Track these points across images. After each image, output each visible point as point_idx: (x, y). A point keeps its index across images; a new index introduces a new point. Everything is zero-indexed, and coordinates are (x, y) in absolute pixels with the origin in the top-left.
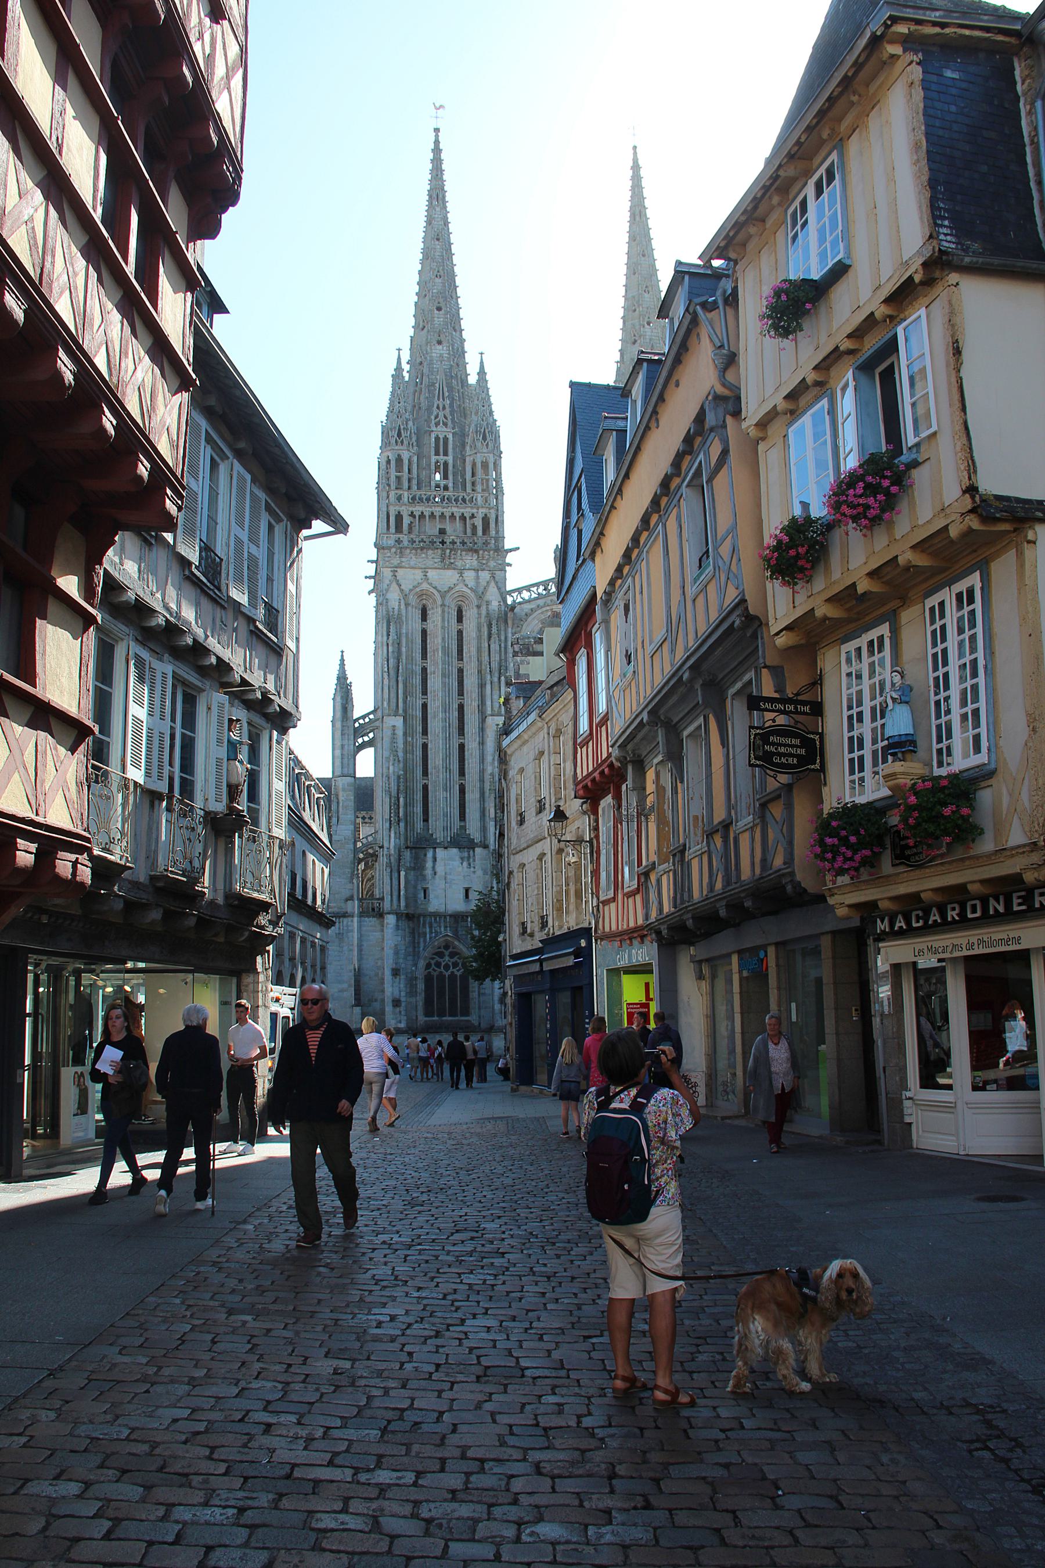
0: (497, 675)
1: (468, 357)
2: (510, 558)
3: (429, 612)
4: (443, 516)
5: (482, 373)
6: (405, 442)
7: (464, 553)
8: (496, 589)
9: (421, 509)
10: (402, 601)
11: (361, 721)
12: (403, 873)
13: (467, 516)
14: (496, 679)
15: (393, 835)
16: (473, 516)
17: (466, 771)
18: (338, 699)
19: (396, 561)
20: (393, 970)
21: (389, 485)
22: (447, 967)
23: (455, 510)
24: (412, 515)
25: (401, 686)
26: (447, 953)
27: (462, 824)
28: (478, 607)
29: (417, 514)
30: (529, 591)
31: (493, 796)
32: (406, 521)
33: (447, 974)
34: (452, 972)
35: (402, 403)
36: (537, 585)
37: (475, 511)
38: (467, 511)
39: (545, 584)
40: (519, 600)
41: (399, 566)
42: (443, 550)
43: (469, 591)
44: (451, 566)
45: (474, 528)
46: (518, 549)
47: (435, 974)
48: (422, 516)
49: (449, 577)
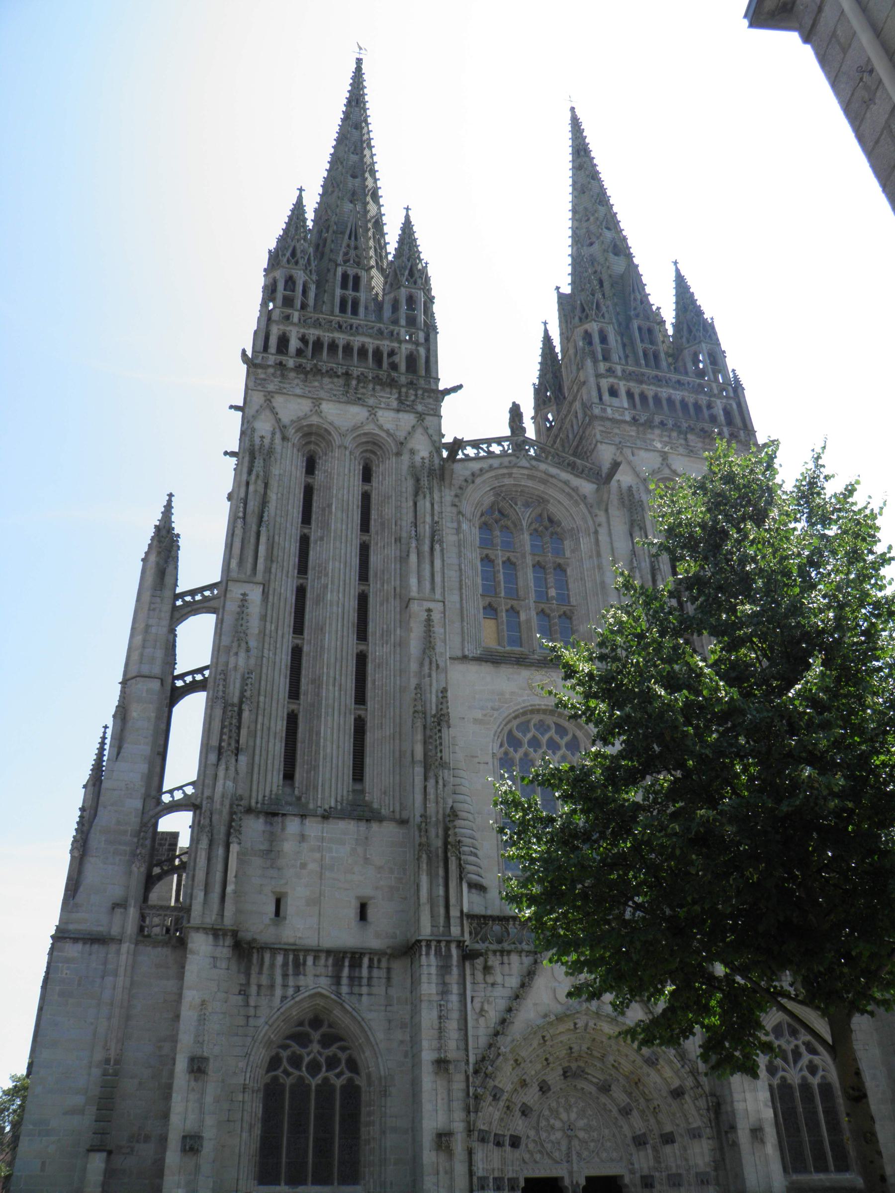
0: (427, 542)
2: (448, 405)
3: (320, 463)
4: (348, 349)
5: (407, 229)
10: (278, 436)
11: (188, 599)
12: (234, 848)
14: (426, 548)
15: (221, 773)
16: (392, 353)
17: (369, 694)
18: (153, 558)
19: (271, 387)
20: (192, 1060)
22: (314, 1068)
23: (367, 340)
24: (303, 339)
25: (263, 539)
26: (316, 1036)
27: (358, 787)
28: (398, 454)
29: (311, 340)
31: (419, 724)
32: (294, 344)
33: (314, 1082)
34: (326, 1080)
36: (489, 441)
38: (386, 345)
39: (499, 441)
41: (280, 392)
43: (384, 435)
44: (359, 401)
45: (394, 367)
46: (460, 387)
47: (289, 1082)
48: (318, 344)
49: (354, 415)
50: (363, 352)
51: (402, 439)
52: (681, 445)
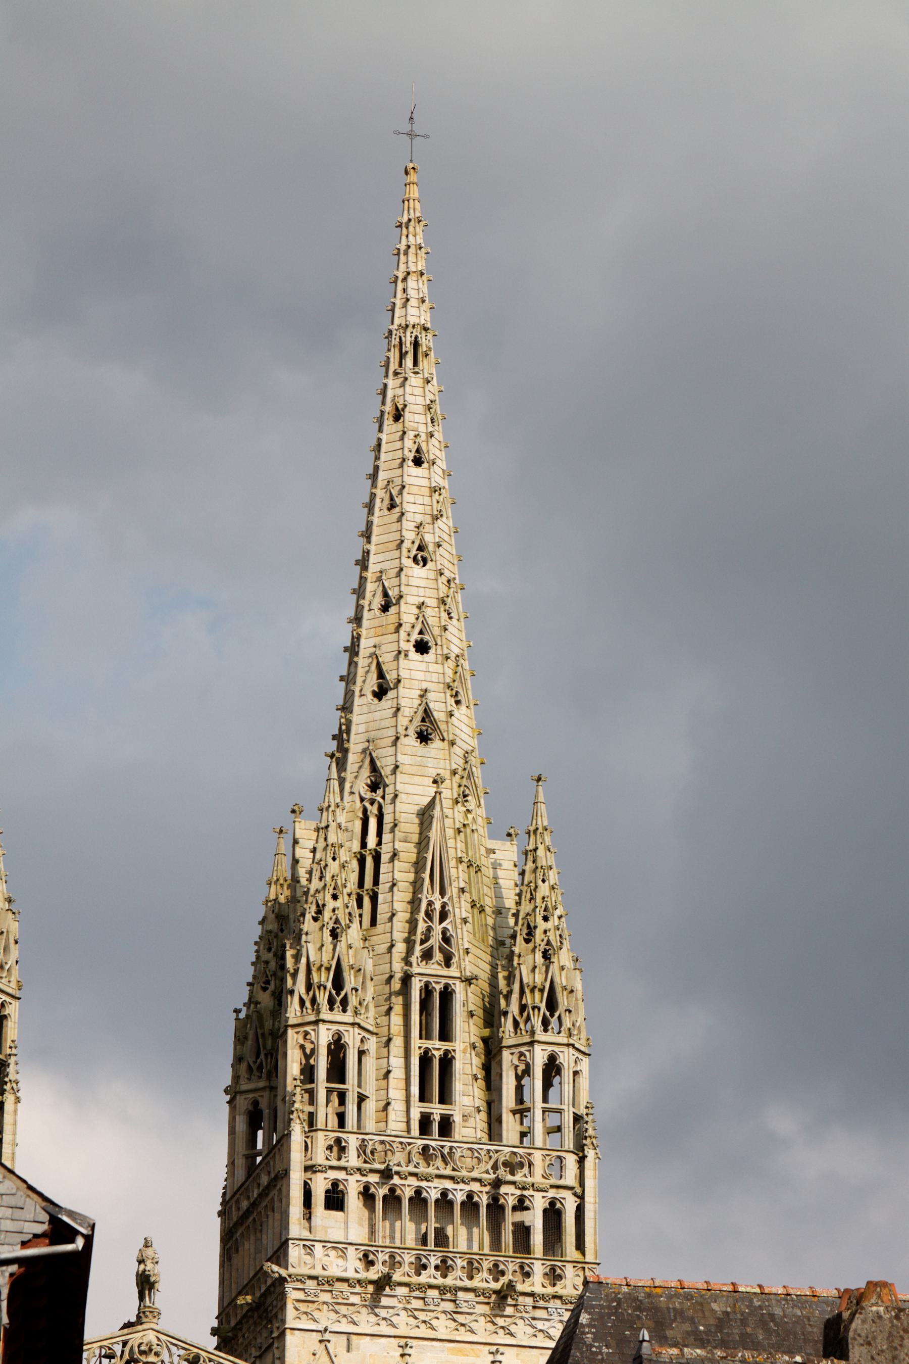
52: (444, 1312)
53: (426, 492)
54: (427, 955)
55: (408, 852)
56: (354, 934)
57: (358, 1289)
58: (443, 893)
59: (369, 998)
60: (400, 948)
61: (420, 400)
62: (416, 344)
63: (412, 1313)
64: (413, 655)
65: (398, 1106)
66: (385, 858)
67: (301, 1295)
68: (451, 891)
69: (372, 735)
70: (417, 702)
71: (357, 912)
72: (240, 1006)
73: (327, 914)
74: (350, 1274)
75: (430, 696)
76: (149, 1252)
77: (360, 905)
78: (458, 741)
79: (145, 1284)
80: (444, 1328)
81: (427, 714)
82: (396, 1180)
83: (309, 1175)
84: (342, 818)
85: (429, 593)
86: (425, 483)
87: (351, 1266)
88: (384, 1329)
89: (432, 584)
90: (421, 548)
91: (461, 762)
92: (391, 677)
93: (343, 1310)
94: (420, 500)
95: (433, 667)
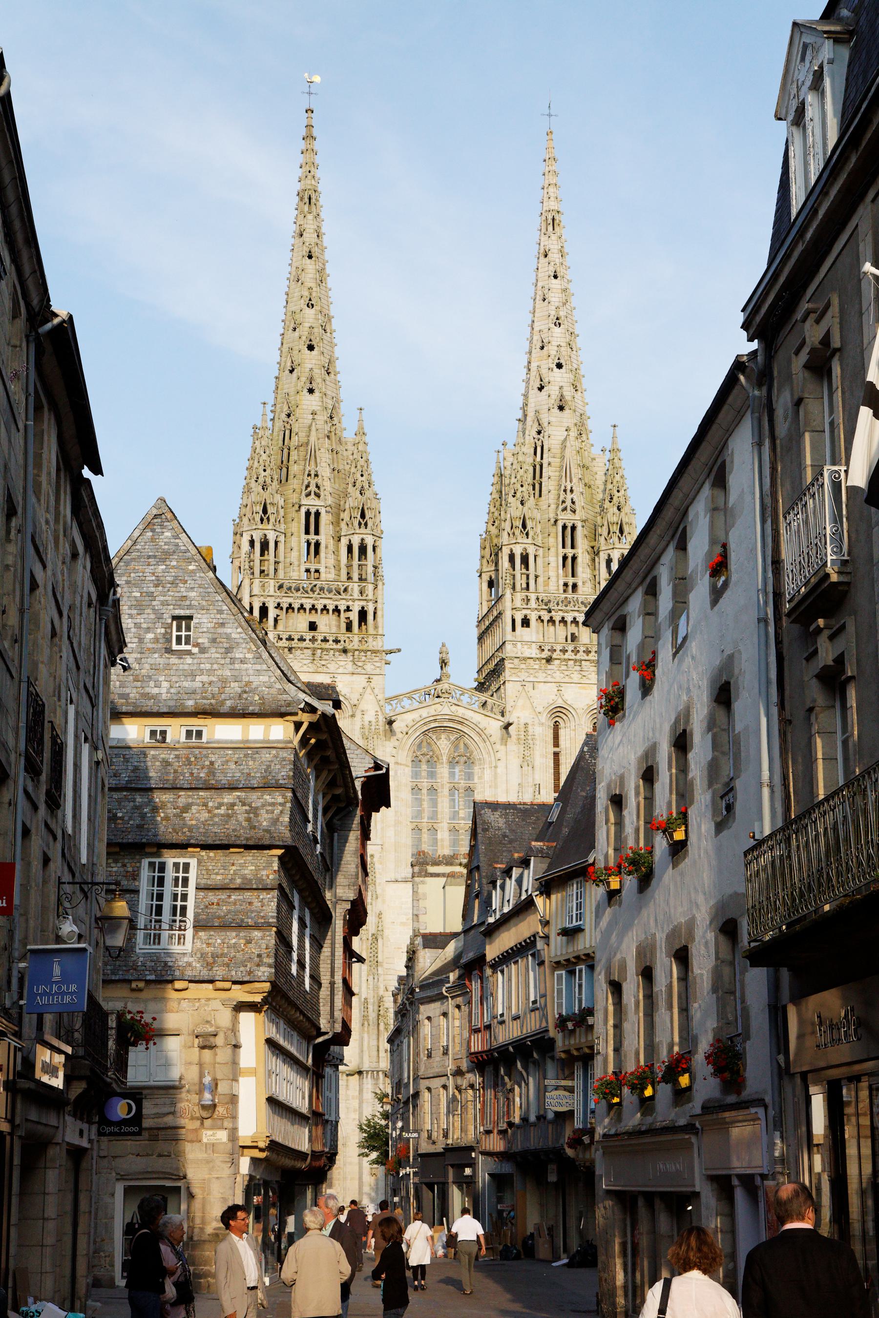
1: (343, 408)
6: (272, 520)
7: (337, 653)
8: (372, 697)
9: (290, 600)
13: (342, 608)
16: (348, 609)
21: (253, 574)
28: (353, 716)
30: (409, 698)
32: (272, 613)
35: (268, 471)
37: (350, 603)
40: (399, 710)
42: (314, 649)
46: (399, 650)
48: (290, 607)
50: (325, 609)
51: (356, 702)
53: (560, 291)
54: (565, 509)
55: (556, 462)
56: (531, 502)
57: (538, 662)
58: (571, 481)
59: (539, 531)
60: (553, 506)
61: (556, 247)
62: (553, 219)
63: (562, 672)
64: (555, 369)
65: (553, 579)
66: (545, 466)
67: (512, 666)
68: (575, 480)
69: (537, 408)
70: (557, 393)
71: (532, 492)
72: (482, 533)
73: (518, 495)
74: (533, 656)
75: (565, 389)
76: (444, 649)
77: (534, 489)
78: (577, 409)
79: (444, 663)
80: (576, 677)
81: (562, 398)
82: (553, 613)
83: (514, 611)
84: (524, 449)
85: (563, 340)
86: (559, 287)
87: (534, 652)
88: (549, 679)
89: (563, 336)
90: (557, 319)
91: (579, 419)
92: (546, 380)
93: (532, 671)
94: (557, 295)
95: (565, 375)
